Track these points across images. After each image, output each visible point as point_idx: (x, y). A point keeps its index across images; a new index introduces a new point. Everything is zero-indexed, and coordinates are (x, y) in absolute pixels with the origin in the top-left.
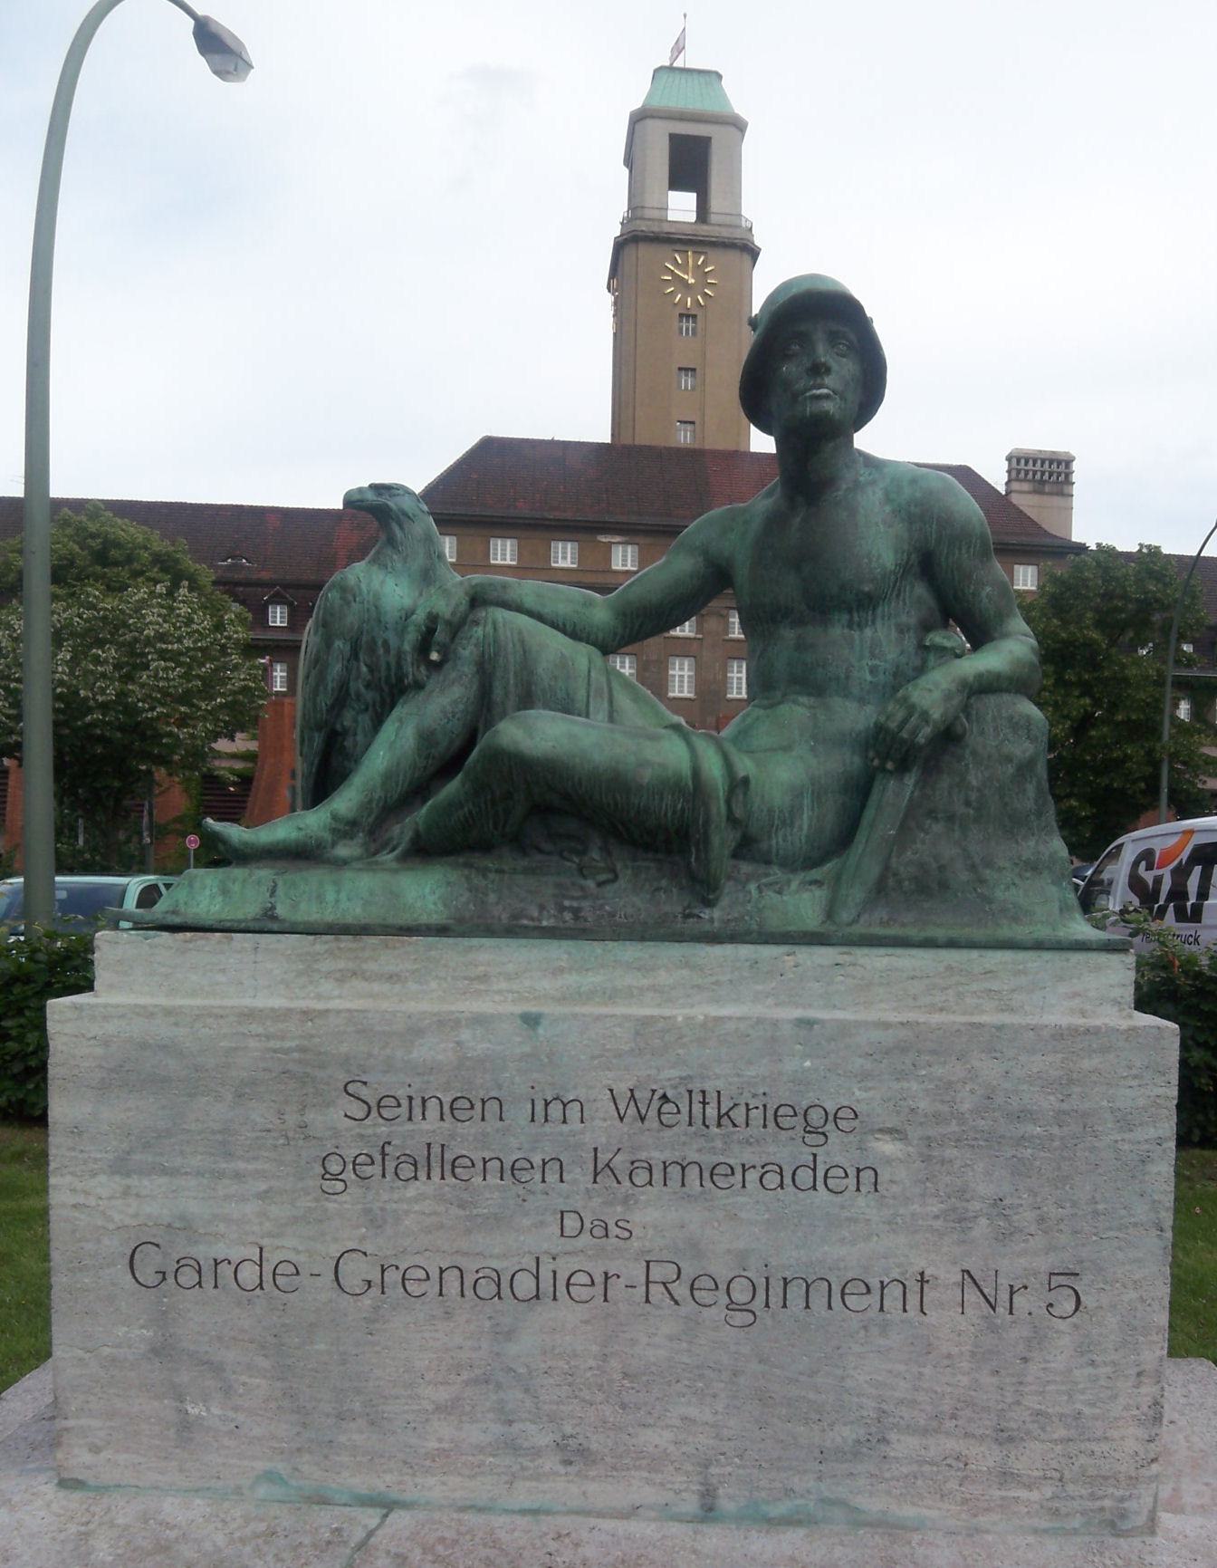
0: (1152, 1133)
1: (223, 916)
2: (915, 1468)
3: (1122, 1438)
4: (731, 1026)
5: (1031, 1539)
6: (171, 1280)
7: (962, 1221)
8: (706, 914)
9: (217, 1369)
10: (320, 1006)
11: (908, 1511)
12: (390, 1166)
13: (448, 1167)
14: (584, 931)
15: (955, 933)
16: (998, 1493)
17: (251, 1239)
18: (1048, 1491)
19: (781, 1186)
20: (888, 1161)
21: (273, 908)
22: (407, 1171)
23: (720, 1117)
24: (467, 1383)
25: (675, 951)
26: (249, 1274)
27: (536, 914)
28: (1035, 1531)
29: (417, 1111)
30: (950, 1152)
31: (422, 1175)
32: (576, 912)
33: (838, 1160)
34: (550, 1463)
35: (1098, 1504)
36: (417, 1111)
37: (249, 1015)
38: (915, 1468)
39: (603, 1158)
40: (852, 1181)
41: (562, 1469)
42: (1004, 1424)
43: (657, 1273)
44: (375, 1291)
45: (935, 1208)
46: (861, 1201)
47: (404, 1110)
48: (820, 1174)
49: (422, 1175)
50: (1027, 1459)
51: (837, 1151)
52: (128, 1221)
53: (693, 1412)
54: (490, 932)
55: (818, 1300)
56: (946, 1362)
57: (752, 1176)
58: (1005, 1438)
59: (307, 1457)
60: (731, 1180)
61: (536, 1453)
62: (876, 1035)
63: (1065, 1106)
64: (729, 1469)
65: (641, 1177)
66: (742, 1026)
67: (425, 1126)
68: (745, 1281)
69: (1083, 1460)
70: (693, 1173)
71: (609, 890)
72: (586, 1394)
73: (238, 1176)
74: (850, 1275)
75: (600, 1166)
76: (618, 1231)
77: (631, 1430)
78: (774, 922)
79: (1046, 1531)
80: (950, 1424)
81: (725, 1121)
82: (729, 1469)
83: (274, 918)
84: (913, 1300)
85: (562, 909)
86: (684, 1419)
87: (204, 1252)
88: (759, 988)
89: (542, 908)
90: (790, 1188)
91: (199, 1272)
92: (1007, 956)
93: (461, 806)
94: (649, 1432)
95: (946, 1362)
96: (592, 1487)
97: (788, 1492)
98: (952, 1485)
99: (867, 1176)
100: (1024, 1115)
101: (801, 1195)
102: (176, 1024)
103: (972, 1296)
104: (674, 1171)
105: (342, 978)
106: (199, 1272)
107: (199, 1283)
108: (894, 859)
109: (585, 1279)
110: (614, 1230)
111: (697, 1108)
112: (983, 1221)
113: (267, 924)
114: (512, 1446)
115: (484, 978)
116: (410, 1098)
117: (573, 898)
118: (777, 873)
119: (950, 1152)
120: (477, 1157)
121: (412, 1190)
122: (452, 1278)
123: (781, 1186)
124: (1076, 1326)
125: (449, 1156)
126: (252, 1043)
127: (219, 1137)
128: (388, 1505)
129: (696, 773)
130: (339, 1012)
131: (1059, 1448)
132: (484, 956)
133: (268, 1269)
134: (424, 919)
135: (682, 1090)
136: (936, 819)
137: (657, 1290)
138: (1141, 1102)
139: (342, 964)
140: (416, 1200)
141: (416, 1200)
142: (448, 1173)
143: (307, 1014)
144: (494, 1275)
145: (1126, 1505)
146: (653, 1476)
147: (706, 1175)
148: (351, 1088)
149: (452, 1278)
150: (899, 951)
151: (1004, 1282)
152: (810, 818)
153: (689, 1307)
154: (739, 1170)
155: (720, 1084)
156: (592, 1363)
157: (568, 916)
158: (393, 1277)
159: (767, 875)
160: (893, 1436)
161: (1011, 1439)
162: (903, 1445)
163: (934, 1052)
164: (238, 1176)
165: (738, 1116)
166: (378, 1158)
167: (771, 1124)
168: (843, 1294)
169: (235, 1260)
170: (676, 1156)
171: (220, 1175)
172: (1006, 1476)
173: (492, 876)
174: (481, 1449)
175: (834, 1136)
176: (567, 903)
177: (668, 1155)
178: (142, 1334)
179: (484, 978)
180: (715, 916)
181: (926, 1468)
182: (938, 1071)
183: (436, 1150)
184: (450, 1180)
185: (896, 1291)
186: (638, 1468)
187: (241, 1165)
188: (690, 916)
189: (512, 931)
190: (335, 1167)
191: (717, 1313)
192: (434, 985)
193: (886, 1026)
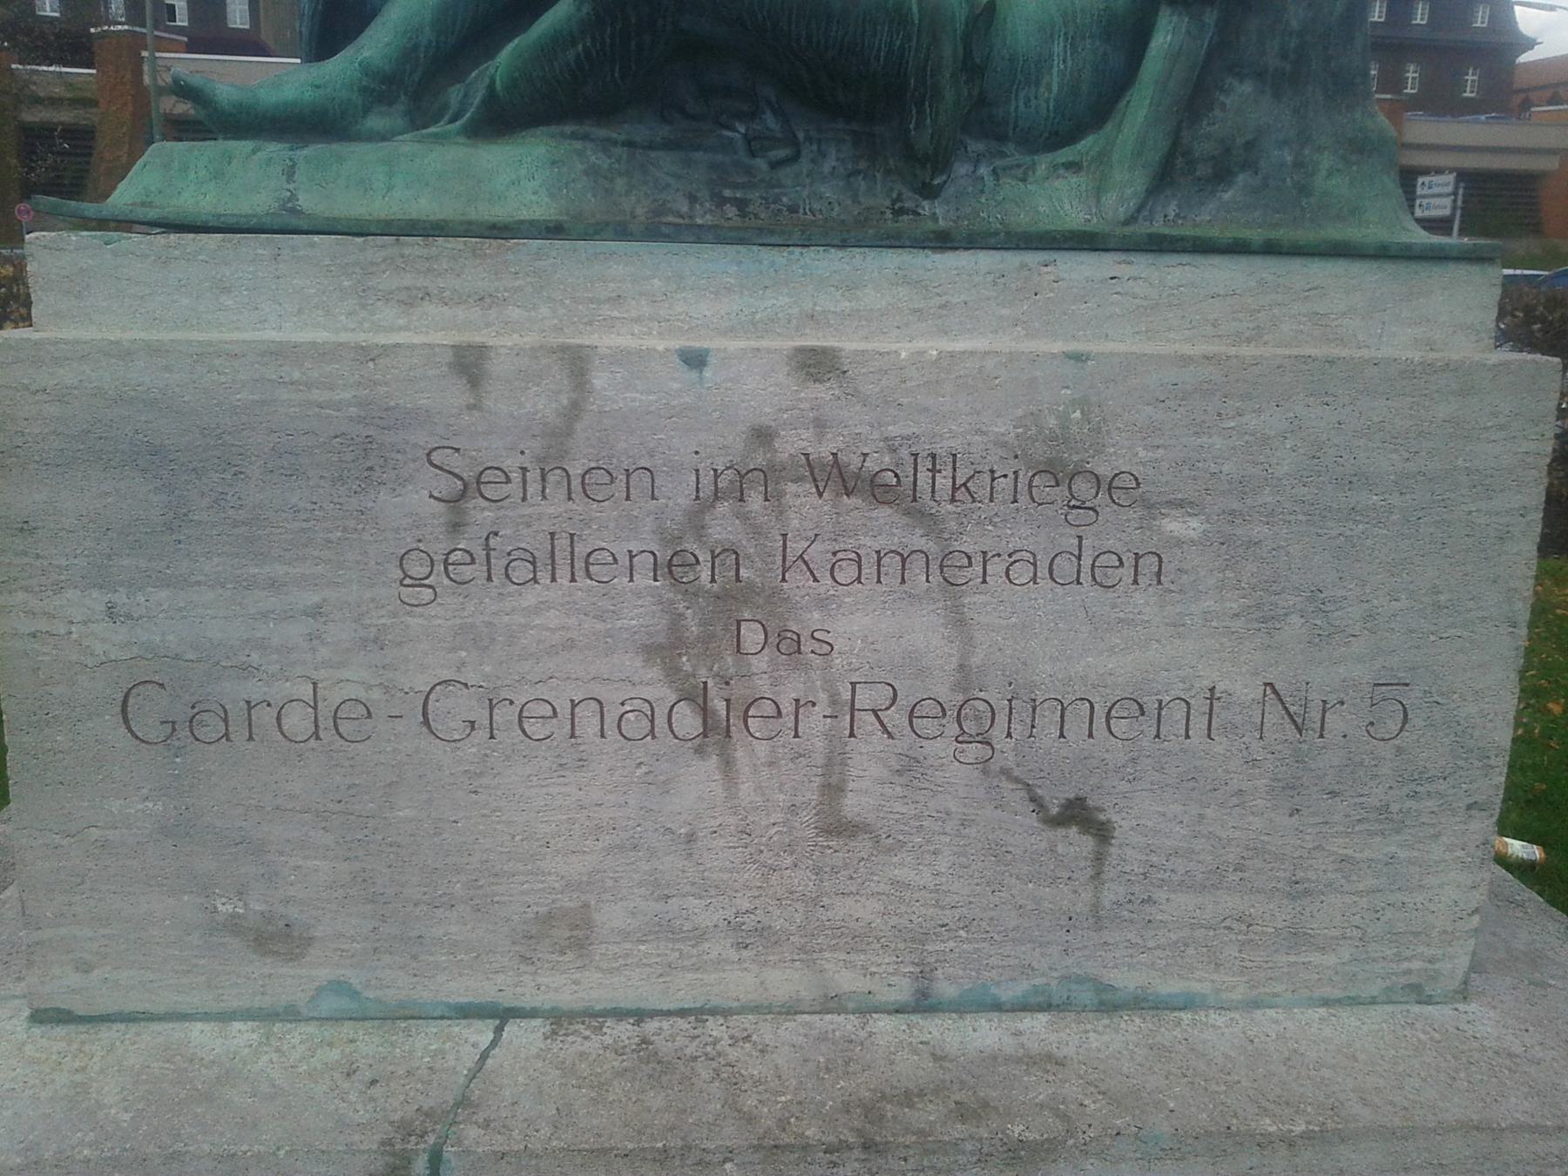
1: (220, 210)
3: (1441, 886)
5: (1322, 1011)
6: (183, 733)
8: (926, 207)
10: (382, 339)
11: (1170, 987)
12: (498, 565)
14: (761, 229)
15: (1283, 234)
16: (1284, 959)
17: (299, 671)
18: (1346, 953)
19: (1034, 579)
20: (1179, 543)
21: (293, 197)
22: (521, 572)
23: (955, 489)
25: (892, 259)
26: (298, 721)
27: (685, 209)
28: (1326, 1003)
29: (533, 488)
30: (1258, 531)
31: (544, 578)
32: (741, 205)
33: (1110, 543)
34: (717, 948)
35: (1405, 965)
36: (533, 488)
37: (279, 352)
39: (796, 547)
40: (1127, 573)
41: (733, 955)
42: (1300, 874)
43: (864, 698)
46: (1139, 598)
47: (514, 488)
48: (1087, 562)
49: (544, 578)
51: (1115, 530)
54: (623, 233)
56: (1235, 800)
57: (997, 567)
58: (1298, 890)
59: (387, 959)
60: (968, 573)
61: (700, 935)
64: (951, 944)
65: (847, 573)
66: (990, 363)
68: (982, 706)
69: (1389, 914)
70: (918, 563)
71: (785, 174)
73: (274, 585)
74: (1119, 694)
75: (790, 558)
76: (816, 645)
77: (826, 901)
78: (1022, 220)
81: (958, 496)
82: (951, 944)
83: (294, 211)
85: (722, 201)
86: (894, 883)
88: (1004, 312)
89: (693, 199)
90: (1044, 583)
91: (226, 720)
92: (1338, 267)
93: (574, 44)
94: (849, 901)
95: (1235, 800)
96: (774, 976)
97: (1027, 969)
101: (1059, 589)
102: (167, 368)
103: (1274, 715)
104: (892, 563)
105: (411, 300)
106: (226, 720)
107: (226, 735)
108: (1185, 133)
109: (769, 709)
111: (924, 478)
112: (1295, 619)
113: (286, 224)
114: (664, 929)
116: (524, 470)
117: (735, 186)
118: (1014, 155)
119: (1258, 531)
121: (530, 597)
122: (587, 713)
123: (1034, 579)
125: (581, 550)
128: (503, 1015)
130: (412, 347)
131: (1364, 902)
133: (325, 712)
134: (525, 215)
135: (904, 453)
136: (1241, 78)
139: (408, 280)
140: (537, 610)
141: (537, 610)
143: (367, 354)
144: (646, 708)
145: (1437, 966)
146: (853, 957)
147: (934, 567)
148: (435, 457)
149: (587, 713)
150: (1199, 259)
151: (1315, 698)
152: (1062, 74)
155: (956, 444)
156: (778, 817)
157: (731, 211)
158: (505, 715)
159: (1003, 155)
160: (1160, 895)
161: (1307, 892)
164: (274, 585)
165: (981, 486)
166: (480, 554)
167: (1023, 499)
168: (1108, 717)
172: (1297, 937)
173: (618, 151)
174: (625, 935)
175: (1107, 512)
176: (727, 193)
177: (881, 542)
180: (938, 213)
181: (1200, 933)
182: (1252, 421)
183: (563, 542)
185: (1179, 711)
186: (834, 949)
187: (280, 570)
188: (903, 211)
189: (653, 233)
190: (418, 570)
191: (940, 749)
192: (544, 310)
193: (1185, 360)
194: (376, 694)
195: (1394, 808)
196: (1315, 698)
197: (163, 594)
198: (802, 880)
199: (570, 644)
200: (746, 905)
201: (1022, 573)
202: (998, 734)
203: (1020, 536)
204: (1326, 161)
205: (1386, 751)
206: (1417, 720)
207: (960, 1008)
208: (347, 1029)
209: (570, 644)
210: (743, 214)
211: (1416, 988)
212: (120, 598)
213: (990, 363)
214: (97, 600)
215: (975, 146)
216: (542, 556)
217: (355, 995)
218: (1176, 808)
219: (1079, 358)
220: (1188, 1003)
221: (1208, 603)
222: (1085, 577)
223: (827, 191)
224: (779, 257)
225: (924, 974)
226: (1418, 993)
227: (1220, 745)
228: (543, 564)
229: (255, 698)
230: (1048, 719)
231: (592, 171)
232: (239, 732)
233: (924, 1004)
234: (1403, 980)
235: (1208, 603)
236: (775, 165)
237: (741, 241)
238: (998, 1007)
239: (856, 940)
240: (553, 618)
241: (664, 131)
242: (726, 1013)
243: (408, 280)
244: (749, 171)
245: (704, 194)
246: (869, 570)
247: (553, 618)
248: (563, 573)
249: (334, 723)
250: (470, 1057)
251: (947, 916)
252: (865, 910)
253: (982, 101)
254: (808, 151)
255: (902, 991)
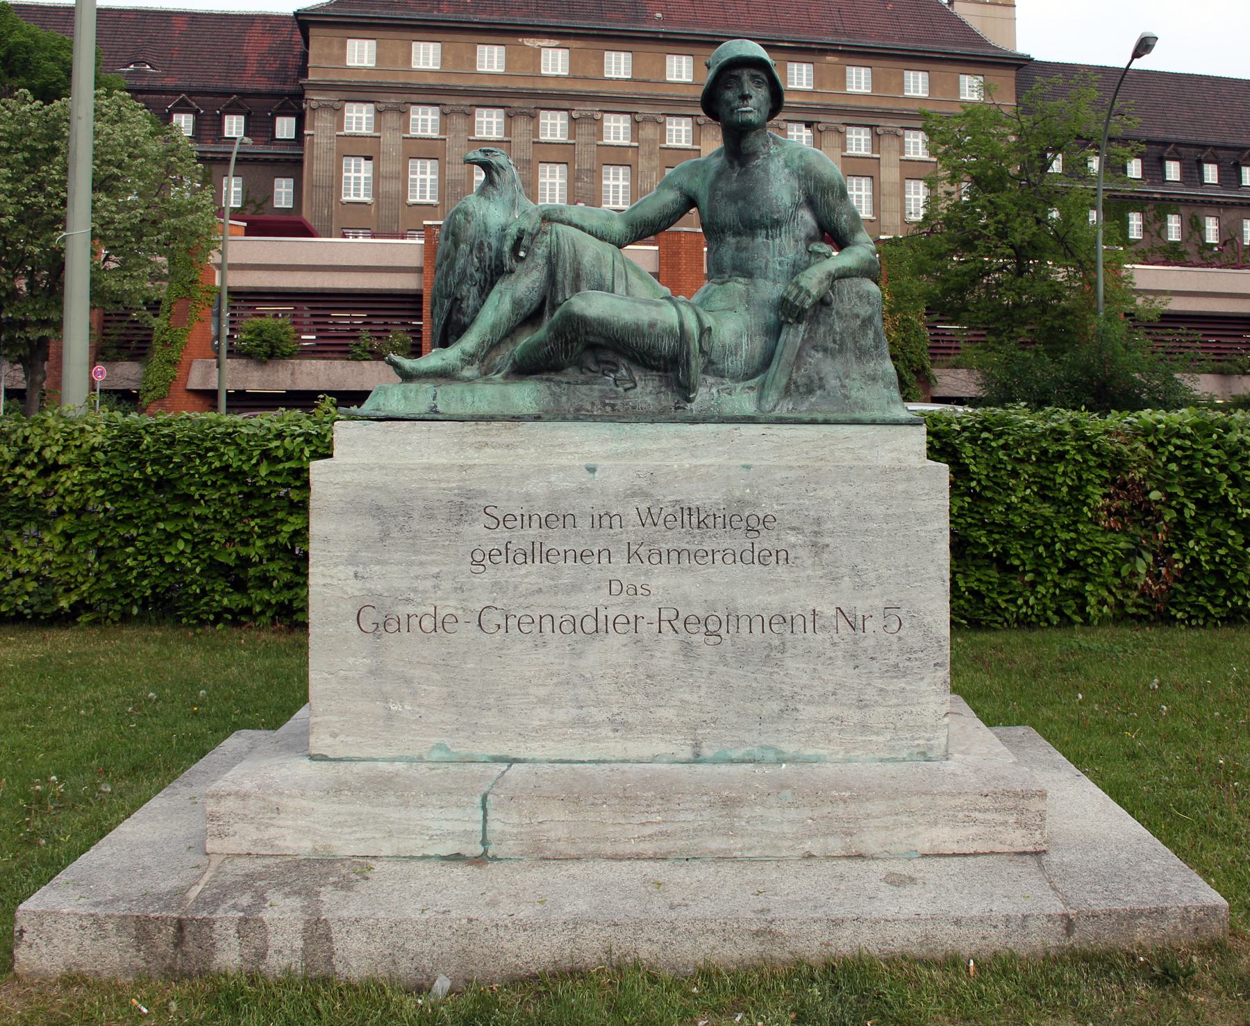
0: (936, 526)
2: (813, 725)
4: (704, 470)
7: (835, 579)
9: (408, 681)
11: (809, 752)
13: (544, 555)
14: (619, 417)
15: (831, 416)
20: (794, 546)
22: (520, 559)
24: (556, 685)
26: (428, 623)
28: (881, 760)
30: (827, 540)
31: (529, 560)
32: (613, 406)
33: (765, 546)
34: (606, 731)
36: (526, 521)
37: (429, 468)
38: (813, 725)
39: (634, 548)
40: (774, 558)
41: (611, 734)
44: (503, 630)
45: (820, 573)
46: (779, 570)
47: (519, 523)
48: (756, 554)
49: (529, 560)
50: (876, 716)
51: (766, 542)
52: (357, 593)
53: (687, 697)
54: (564, 419)
55: (757, 628)
58: (862, 704)
59: (462, 734)
61: (597, 725)
62: (784, 474)
63: (890, 512)
65: (655, 559)
66: (711, 470)
67: (531, 532)
69: (906, 716)
72: (626, 689)
73: (421, 564)
79: (888, 760)
80: (832, 698)
81: (702, 525)
84: (810, 626)
85: (605, 405)
86: (682, 701)
87: (403, 610)
89: (593, 404)
96: (630, 745)
98: (835, 734)
99: (782, 555)
100: (867, 517)
103: (842, 622)
104: (674, 555)
105: (480, 446)
110: (640, 591)
112: (846, 579)
114: (582, 722)
115: (562, 445)
120: (561, 550)
121: (524, 570)
122: (547, 622)
124: (900, 638)
125: (545, 549)
126: (430, 485)
127: (410, 541)
128: (512, 761)
129: (681, 325)
131: (893, 710)
132: (562, 433)
133: (439, 619)
134: (525, 412)
135: (677, 507)
137: (665, 625)
138: (930, 509)
140: (526, 576)
141: (526, 576)
142: (544, 560)
147: (692, 557)
149: (547, 622)
151: (859, 614)
153: (683, 635)
154: (710, 553)
160: (800, 707)
161: (866, 706)
162: (807, 712)
163: (817, 483)
164: (421, 564)
165: (710, 521)
166: (504, 551)
167: (728, 527)
169: (420, 615)
170: (675, 546)
171: (411, 564)
172: (864, 727)
174: (564, 724)
177: (670, 546)
178: (363, 662)
179: (562, 445)
181: (820, 725)
183: (537, 546)
184: (545, 563)
186: (656, 732)
187: (423, 558)
190: (478, 558)
191: (699, 638)
193: (791, 468)
194: (460, 612)
195: (901, 665)
196: (859, 614)
197: (377, 568)
198: (639, 699)
199: (540, 591)
200: (616, 711)
201: (729, 559)
202: (723, 631)
203: (726, 543)
204: (857, 384)
205: (894, 639)
206: (906, 624)
207: (715, 761)
208: (444, 765)
209: (540, 591)
210: (613, 410)
211: (923, 754)
212: (360, 569)
213: (711, 470)
214: (351, 570)
215: (710, 380)
216: (529, 553)
217: (448, 750)
218: (803, 666)
219: (748, 467)
220: (818, 760)
221: (809, 572)
222: (756, 560)
223: (648, 399)
224: (627, 427)
225: (697, 745)
226: (925, 756)
227: (820, 636)
228: (529, 555)
229: (411, 613)
230: (744, 623)
231: (553, 394)
232: (404, 628)
233: (697, 759)
234: (916, 750)
235: (809, 572)
236: (626, 390)
237: (611, 421)
238: (732, 761)
239: (666, 729)
240: (532, 579)
241: (582, 377)
242: (610, 762)
243: (479, 439)
244: (616, 392)
245: (598, 402)
246: (665, 557)
247: (532, 579)
248: (537, 559)
249: (441, 625)
250: (497, 773)
251: (706, 717)
252: (667, 714)
253: (711, 362)
254: (640, 384)
255: (687, 753)
